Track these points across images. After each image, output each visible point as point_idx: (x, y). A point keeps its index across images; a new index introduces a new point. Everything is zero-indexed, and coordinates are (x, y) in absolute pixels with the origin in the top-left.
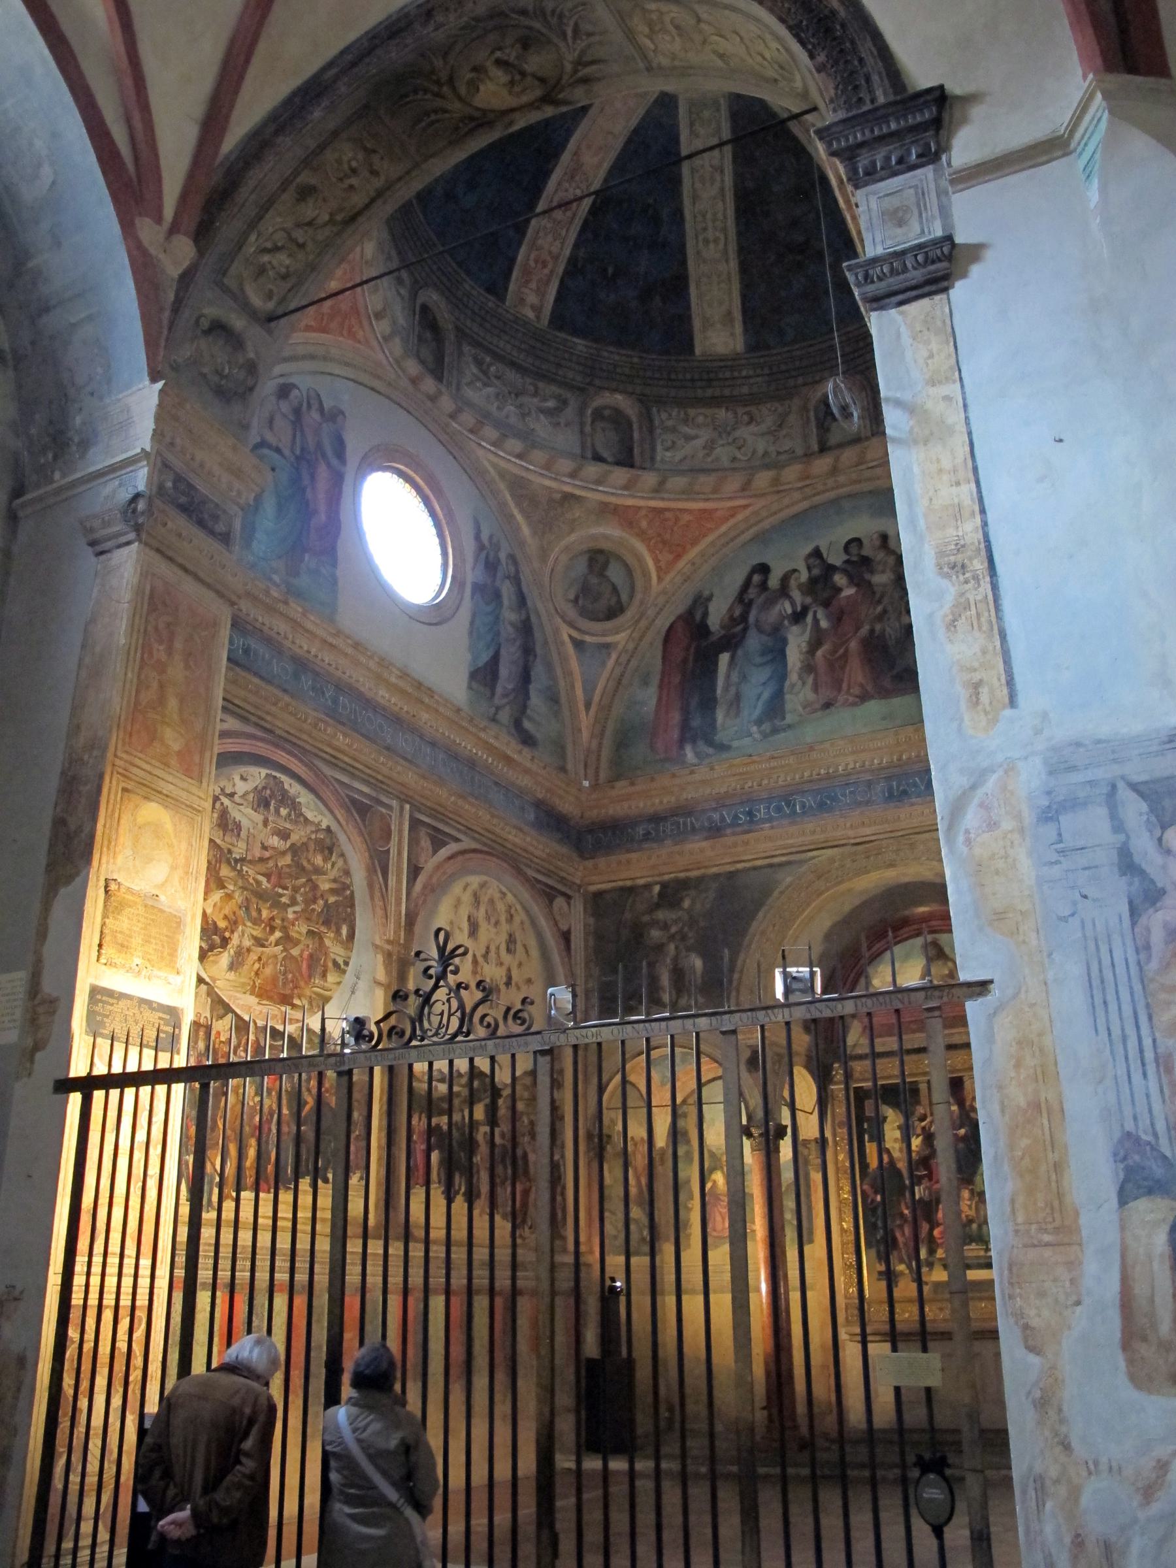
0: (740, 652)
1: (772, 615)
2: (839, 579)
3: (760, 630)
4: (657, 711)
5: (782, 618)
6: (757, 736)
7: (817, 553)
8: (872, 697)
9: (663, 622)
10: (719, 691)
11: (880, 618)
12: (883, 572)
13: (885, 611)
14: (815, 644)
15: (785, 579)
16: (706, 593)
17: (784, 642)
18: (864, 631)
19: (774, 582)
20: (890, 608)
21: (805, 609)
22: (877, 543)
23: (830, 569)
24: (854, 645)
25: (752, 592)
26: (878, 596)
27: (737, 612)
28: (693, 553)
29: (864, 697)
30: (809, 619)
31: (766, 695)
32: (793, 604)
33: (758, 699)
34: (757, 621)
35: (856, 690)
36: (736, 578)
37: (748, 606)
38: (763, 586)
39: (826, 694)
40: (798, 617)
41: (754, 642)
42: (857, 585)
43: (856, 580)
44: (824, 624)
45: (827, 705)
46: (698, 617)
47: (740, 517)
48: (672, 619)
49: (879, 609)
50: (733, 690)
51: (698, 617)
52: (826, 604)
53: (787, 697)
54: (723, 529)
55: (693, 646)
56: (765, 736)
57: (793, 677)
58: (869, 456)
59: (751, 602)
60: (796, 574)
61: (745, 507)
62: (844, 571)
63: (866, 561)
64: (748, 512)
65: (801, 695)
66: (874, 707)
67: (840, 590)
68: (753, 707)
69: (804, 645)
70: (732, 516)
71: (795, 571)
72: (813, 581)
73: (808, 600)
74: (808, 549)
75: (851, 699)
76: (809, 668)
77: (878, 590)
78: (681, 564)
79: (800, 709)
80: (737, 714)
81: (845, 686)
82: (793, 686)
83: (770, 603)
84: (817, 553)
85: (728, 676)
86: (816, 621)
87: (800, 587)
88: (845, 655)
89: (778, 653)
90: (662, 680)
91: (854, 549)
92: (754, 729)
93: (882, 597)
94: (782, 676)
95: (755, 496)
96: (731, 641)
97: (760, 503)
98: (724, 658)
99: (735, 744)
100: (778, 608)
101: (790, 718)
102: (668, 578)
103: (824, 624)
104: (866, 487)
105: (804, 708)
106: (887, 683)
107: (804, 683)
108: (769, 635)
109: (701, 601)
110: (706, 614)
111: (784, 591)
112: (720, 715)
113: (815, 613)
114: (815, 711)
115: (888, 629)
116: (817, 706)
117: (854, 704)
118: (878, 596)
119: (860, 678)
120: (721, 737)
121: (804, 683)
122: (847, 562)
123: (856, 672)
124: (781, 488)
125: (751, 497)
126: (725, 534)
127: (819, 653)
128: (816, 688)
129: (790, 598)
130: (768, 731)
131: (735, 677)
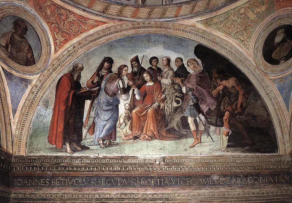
0: (96, 102)
1: (112, 87)
2: (146, 76)
3: (107, 93)
4: (52, 122)
5: (118, 88)
6: (102, 146)
7: (136, 59)
8: (156, 138)
9: (57, 76)
10: (84, 120)
11: (163, 100)
12: (167, 78)
13: (166, 98)
14: (133, 106)
15: (121, 69)
16: (80, 65)
17: (118, 102)
18: (156, 105)
19: (115, 69)
20: (168, 98)
21: (129, 88)
22: (165, 63)
23: (142, 70)
24: (150, 110)
25: (104, 72)
26: (163, 89)
27: (96, 80)
28: (75, 40)
29: (152, 138)
30: (131, 92)
31: (107, 126)
32: (123, 83)
33: (104, 127)
34: (105, 87)
35: (149, 134)
36: (96, 62)
37: (101, 78)
38: (109, 70)
39: (137, 133)
40: (126, 91)
41: (103, 97)
42: (153, 81)
43: (154, 78)
44: (137, 97)
45: (136, 138)
46: (75, 77)
47: (99, 28)
48: (61, 75)
49: (163, 96)
50: (91, 120)
51: (75, 77)
52: (139, 88)
53: (117, 129)
54: (91, 32)
55: (73, 92)
56: (106, 146)
57: (121, 120)
58: (168, 14)
59: (103, 76)
60: (126, 68)
61: (104, 23)
62: (149, 73)
63: (159, 70)
64: (104, 26)
65: (124, 130)
66: (156, 142)
67: (146, 82)
68: (101, 132)
69: (127, 105)
70: (97, 26)
71: (125, 66)
72: (134, 74)
73: (131, 83)
74: (133, 56)
75: (147, 137)
76: (129, 117)
77: (164, 87)
78: (67, 45)
79: (124, 136)
80: (93, 132)
81: (144, 131)
82: (121, 124)
83: (112, 80)
84: (136, 59)
85: (89, 113)
86: (134, 95)
87: (127, 75)
88: (146, 115)
89: (114, 107)
90: (55, 106)
91: (154, 63)
92: (101, 142)
93: (165, 90)
94: (116, 119)
95: (109, 18)
96: (92, 95)
97: (111, 24)
98: (88, 103)
99: (91, 147)
100: (116, 83)
101: (118, 140)
102: (60, 51)
103: (137, 97)
104: (163, 31)
105: (125, 136)
106: (164, 133)
107: (126, 125)
108: (111, 96)
109: (76, 70)
110: (79, 77)
111: (119, 75)
112: (84, 131)
113: (134, 90)
114: (131, 139)
115: (166, 107)
116: (131, 137)
117: (147, 140)
118: (163, 89)
119: (152, 128)
120: (84, 142)
121: (126, 125)
122: (150, 68)
123: (150, 125)
124: (122, 18)
125: (106, 17)
126: (91, 35)
127: (134, 111)
128: (131, 128)
129: (122, 80)
130: (107, 144)
131: (92, 114)
